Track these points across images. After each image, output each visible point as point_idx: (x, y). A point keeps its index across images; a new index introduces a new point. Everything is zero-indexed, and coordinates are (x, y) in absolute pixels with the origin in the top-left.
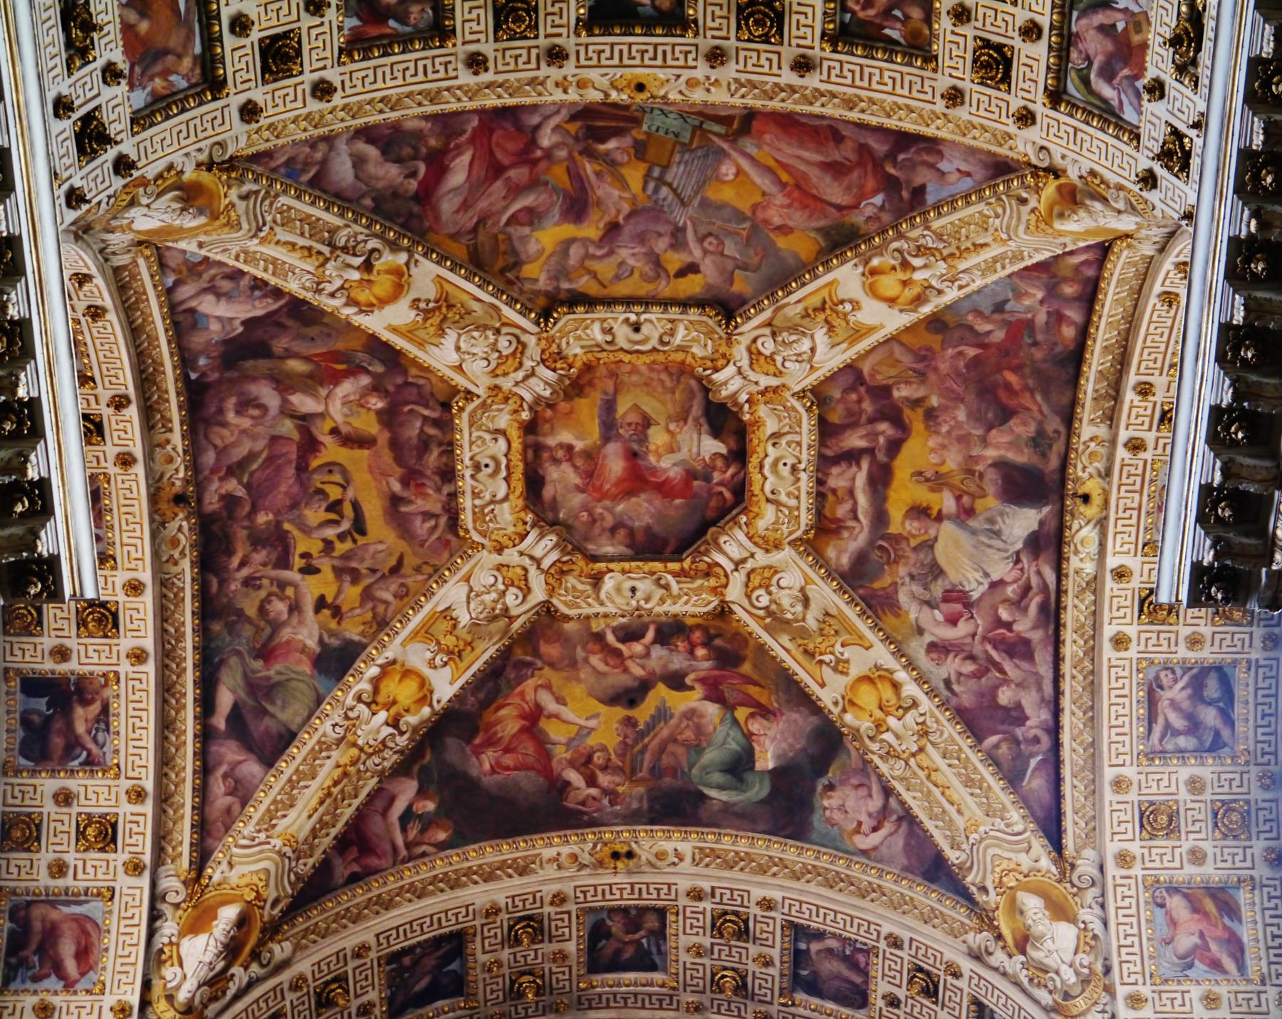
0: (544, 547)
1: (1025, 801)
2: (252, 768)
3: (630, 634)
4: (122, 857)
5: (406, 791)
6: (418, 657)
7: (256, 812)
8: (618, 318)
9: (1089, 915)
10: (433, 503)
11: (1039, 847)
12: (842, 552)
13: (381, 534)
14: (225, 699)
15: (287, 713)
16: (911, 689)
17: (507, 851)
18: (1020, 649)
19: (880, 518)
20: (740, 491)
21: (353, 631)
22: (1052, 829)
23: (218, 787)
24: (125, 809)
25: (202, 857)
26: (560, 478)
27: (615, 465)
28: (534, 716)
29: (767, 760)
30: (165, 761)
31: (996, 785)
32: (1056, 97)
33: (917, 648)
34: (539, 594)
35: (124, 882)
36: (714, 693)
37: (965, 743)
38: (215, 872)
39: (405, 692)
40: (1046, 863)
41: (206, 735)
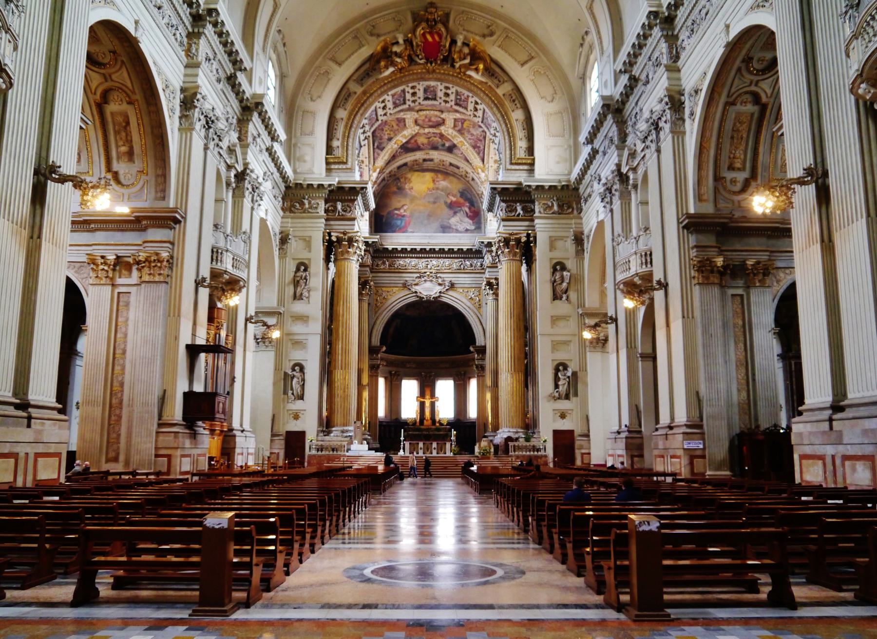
0: (418, 128)
1: (480, 157)
2: (380, 152)
3: (429, 133)
4: (364, 165)
5: (399, 150)
6: (401, 139)
7: (381, 157)
8: (428, 112)
9: (486, 172)
10: (402, 124)
11: (481, 163)
12: (457, 129)
13: (395, 127)
14: (376, 145)
15: (383, 145)
16: (466, 143)
17: (412, 154)
18: (481, 140)
19: (462, 126)
20: (444, 123)
21: (392, 136)
22: (483, 160)
23: (376, 154)
24: (364, 159)
25: (374, 162)
26: (420, 122)
27: (427, 120)
28: (416, 141)
29: (447, 144)
30: (369, 153)
31: (476, 155)
32: (482, 122)
33: (467, 139)
34: (416, 131)
35: (365, 168)
36: (440, 138)
37: (473, 150)
38: (376, 165)
39: (399, 142)
40: (482, 165)
41: (374, 149)
